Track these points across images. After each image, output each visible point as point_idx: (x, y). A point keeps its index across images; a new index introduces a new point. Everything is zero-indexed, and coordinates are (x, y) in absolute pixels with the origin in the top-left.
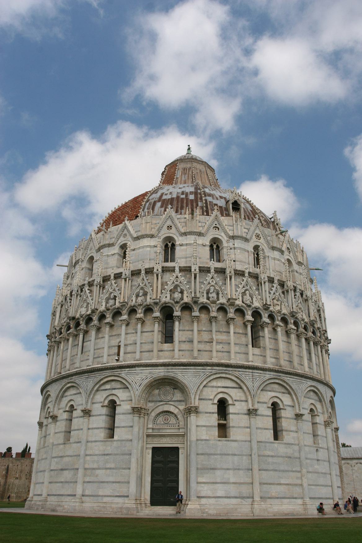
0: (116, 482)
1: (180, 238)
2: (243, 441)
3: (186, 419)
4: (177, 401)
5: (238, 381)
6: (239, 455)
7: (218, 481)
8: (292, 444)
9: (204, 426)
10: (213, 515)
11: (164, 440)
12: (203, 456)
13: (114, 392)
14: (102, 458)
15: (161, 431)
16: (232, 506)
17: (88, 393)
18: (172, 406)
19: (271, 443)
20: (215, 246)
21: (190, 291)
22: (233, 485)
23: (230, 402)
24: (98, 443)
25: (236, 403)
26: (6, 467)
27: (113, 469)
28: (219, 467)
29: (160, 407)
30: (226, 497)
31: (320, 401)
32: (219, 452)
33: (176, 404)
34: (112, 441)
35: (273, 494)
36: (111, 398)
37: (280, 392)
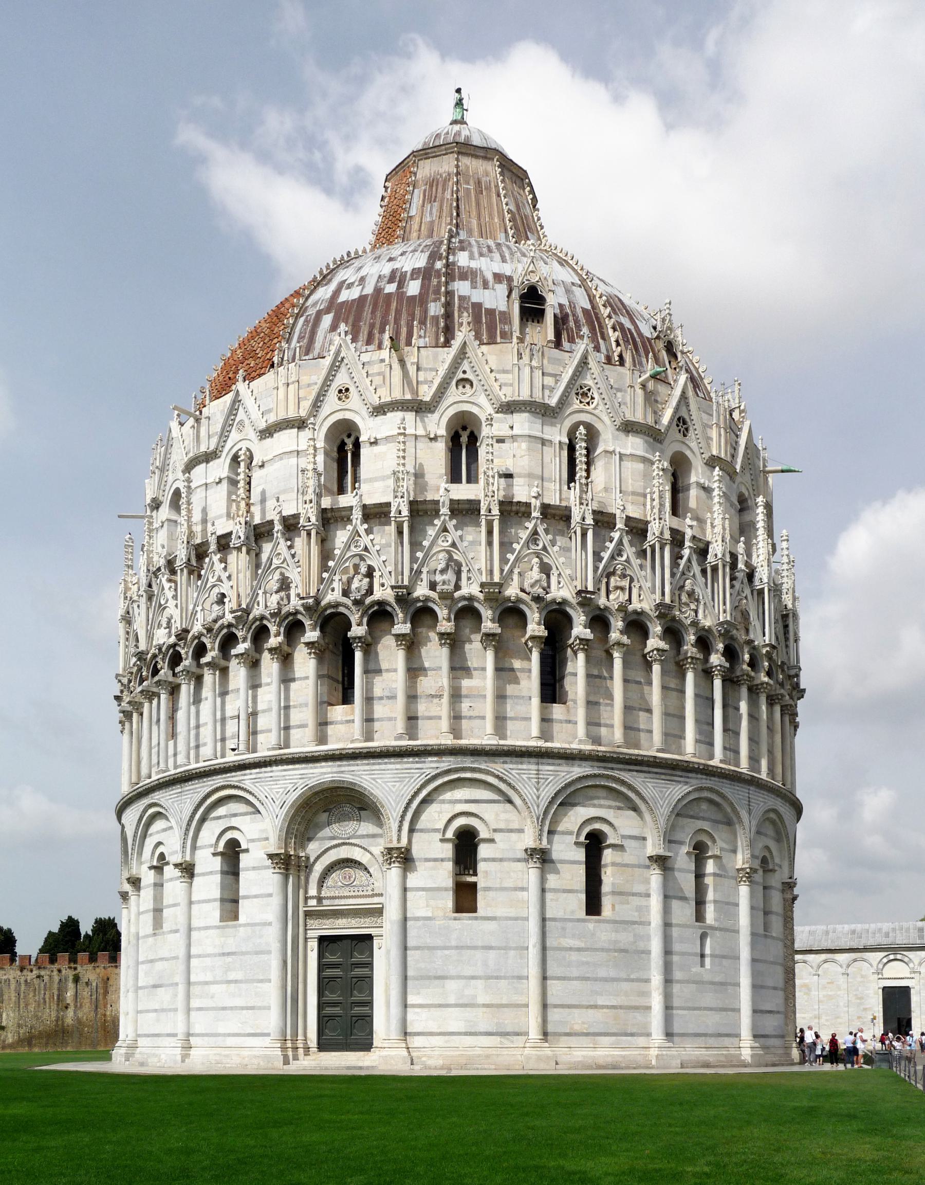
0: (248, 1008)
2: (511, 919)
4: (368, 836)
5: (503, 786)
6: (499, 948)
9: (423, 889)
10: (436, 1068)
11: (342, 922)
12: (418, 952)
14: (219, 961)
15: (337, 902)
16: (478, 1051)
19: (579, 920)
20: (464, 439)
22: (485, 1009)
23: (483, 834)
25: (497, 837)
27: (241, 982)
28: (453, 972)
29: (331, 852)
30: (466, 1034)
32: (454, 943)
34: (235, 926)
35: (577, 1028)
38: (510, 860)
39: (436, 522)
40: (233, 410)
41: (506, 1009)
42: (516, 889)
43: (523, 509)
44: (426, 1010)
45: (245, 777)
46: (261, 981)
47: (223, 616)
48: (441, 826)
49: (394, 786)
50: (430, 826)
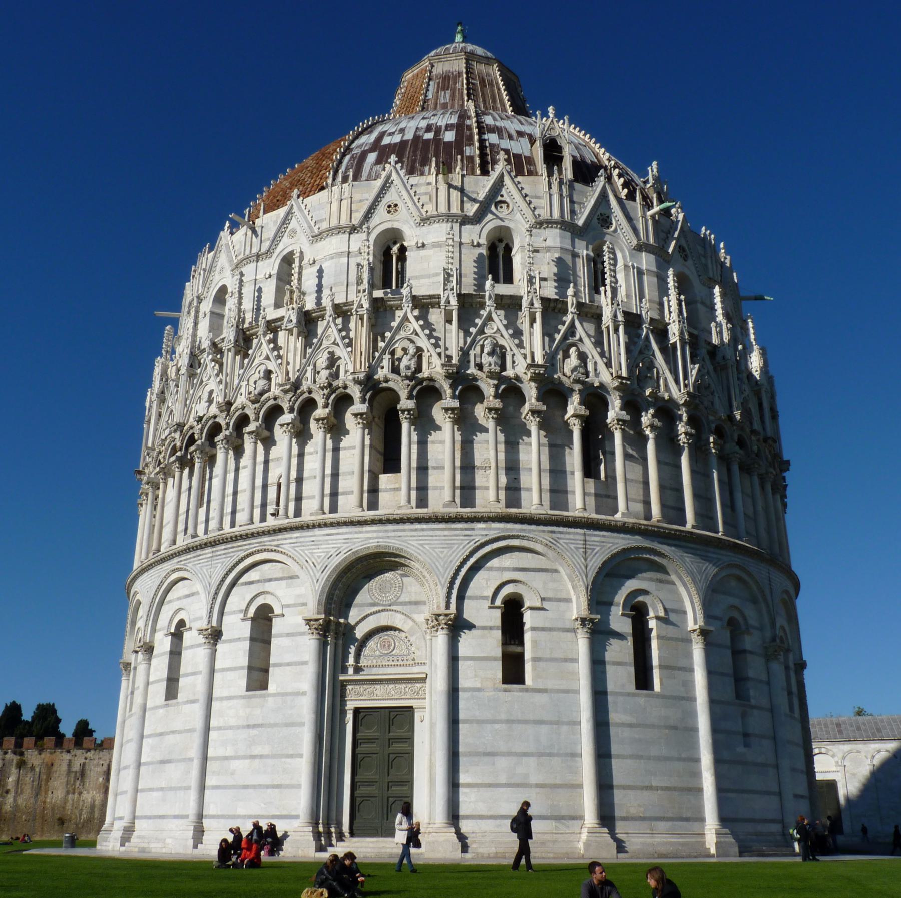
1: (418, 231)
3: (428, 642)
4: (410, 603)
6: (551, 723)
7: (503, 780)
8: (683, 698)
13: (268, 586)
17: (213, 591)
18: (399, 615)
19: (629, 694)
21: (438, 350)
22: (538, 790)
24: (235, 702)
25: (546, 605)
26: (105, 768)
31: (755, 601)
32: (503, 717)
33: (406, 609)
34: (264, 696)
36: (260, 601)
37: (651, 580)
38: (558, 629)
39: (482, 312)
40: (286, 220)
41: (560, 790)
42: (566, 660)
43: (559, 306)
44: (475, 790)
45: (284, 542)
46: (291, 756)
47: (269, 390)
48: (490, 593)
49: (442, 552)
50: (478, 593)
